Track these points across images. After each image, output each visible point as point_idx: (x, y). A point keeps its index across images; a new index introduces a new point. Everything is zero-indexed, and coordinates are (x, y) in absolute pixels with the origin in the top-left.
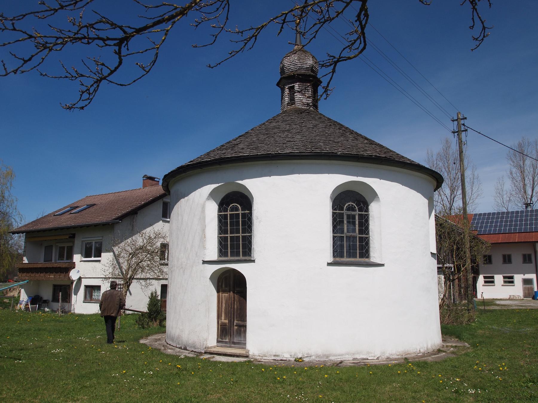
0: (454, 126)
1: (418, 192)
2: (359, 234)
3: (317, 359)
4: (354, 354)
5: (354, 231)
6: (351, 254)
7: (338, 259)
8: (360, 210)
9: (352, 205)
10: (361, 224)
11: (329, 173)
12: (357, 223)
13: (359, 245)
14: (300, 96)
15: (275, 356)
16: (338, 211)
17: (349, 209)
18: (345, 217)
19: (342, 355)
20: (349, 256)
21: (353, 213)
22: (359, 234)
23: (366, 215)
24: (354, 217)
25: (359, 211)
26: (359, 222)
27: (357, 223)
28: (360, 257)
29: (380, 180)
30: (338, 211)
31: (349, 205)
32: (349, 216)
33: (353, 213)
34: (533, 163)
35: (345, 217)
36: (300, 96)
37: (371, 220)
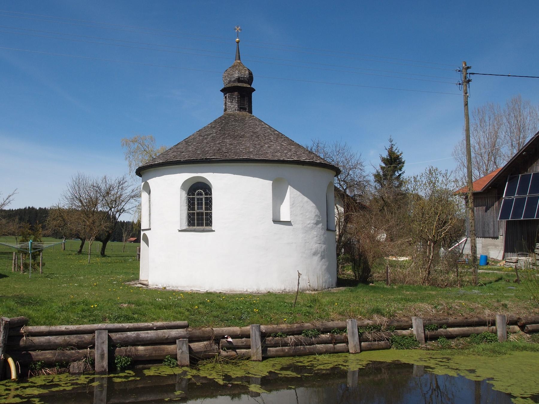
0: (460, 78)
1: (254, 177)
2: (205, 210)
3: (173, 289)
4: (191, 287)
5: (202, 208)
6: (200, 224)
7: (191, 227)
8: (206, 194)
9: (201, 192)
10: (206, 204)
11: (180, 173)
12: (204, 203)
13: (205, 218)
14: (229, 104)
15: (156, 285)
16: (191, 197)
17: (198, 194)
18: (196, 200)
19: (184, 287)
20: (198, 225)
21: (201, 197)
22: (205, 210)
23: (210, 197)
24: (202, 199)
25: (205, 195)
26: (205, 202)
27: (204, 203)
28: (205, 226)
29: (45, 208)
30: (191, 197)
31: (198, 192)
32: (198, 199)
33: (201, 197)
34: (113, 192)
35: (196, 200)
36: (229, 104)
37: (508, 157)
